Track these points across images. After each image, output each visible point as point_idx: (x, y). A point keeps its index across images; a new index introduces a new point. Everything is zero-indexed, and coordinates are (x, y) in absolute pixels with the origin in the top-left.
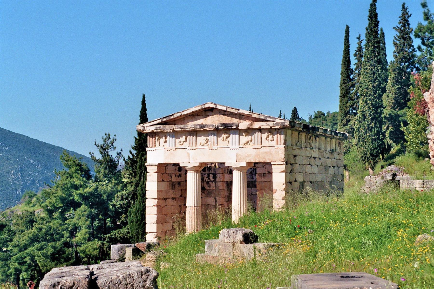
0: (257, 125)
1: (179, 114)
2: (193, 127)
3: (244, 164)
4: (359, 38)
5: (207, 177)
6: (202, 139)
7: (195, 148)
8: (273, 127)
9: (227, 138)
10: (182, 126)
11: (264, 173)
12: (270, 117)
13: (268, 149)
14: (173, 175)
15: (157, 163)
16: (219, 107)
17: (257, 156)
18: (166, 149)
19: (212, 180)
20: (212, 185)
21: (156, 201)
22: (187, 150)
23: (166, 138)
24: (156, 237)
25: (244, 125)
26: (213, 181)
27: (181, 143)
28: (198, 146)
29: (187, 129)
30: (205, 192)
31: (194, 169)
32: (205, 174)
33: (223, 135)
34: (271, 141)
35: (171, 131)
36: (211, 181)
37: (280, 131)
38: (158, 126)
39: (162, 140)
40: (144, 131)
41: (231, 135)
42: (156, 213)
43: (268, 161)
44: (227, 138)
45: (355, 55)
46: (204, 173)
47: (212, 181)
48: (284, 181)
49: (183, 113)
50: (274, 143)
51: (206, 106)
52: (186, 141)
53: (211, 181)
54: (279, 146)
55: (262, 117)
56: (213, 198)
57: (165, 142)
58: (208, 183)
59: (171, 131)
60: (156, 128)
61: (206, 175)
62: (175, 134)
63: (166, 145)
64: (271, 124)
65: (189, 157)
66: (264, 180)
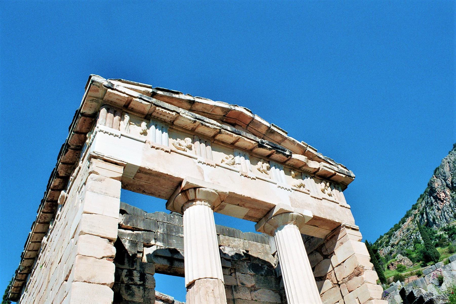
5: (126, 276)
11: (235, 284)
16: (257, 118)
19: (139, 283)
20: (138, 292)
23: (148, 127)
26: (140, 285)
27: (183, 148)
29: (207, 124)
31: (213, 200)
36: (135, 284)
39: (136, 130)
40: (109, 90)
42: (112, 279)
47: (139, 286)
49: (197, 100)
65: (202, 175)
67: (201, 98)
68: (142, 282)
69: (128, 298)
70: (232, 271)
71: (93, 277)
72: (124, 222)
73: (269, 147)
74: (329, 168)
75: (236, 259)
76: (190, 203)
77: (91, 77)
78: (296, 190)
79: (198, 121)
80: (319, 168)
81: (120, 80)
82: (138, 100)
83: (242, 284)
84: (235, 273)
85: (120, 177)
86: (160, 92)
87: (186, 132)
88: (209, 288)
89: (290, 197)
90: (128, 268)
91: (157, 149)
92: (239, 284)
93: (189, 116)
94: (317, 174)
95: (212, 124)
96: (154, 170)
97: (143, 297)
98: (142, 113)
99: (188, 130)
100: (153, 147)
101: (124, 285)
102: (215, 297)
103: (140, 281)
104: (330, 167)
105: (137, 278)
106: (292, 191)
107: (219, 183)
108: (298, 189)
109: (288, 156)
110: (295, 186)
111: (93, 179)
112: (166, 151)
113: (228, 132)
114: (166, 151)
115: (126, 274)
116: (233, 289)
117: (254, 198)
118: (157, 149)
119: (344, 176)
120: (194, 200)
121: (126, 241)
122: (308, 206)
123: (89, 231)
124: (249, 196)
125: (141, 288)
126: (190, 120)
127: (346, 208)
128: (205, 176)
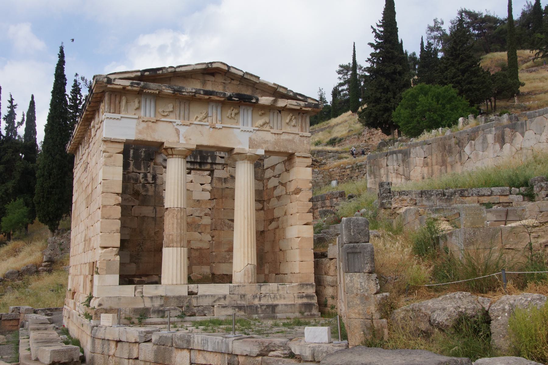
0: (282, 103)
1: (173, 69)
2: (194, 91)
3: (261, 152)
4: (11, 101)
5: (143, 178)
8: (304, 109)
9: (236, 114)
11: (226, 177)
12: (300, 95)
13: (290, 137)
15: (124, 138)
18: (141, 120)
19: (151, 182)
20: (151, 189)
21: (120, 198)
22: (175, 124)
24: (117, 255)
25: (265, 100)
26: (152, 183)
27: (166, 114)
29: (184, 93)
30: (140, 198)
31: (184, 153)
32: (139, 173)
33: (229, 112)
34: (294, 126)
35: (157, 92)
36: (149, 183)
37: (305, 115)
38: (134, 81)
40: (109, 86)
41: (241, 112)
42: (119, 216)
44: (236, 114)
45: (4, 119)
49: (178, 70)
53: (149, 183)
55: (291, 94)
56: (152, 208)
58: (144, 186)
59: (157, 92)
60: (132, 83)
61: (141, 175)
65: (178, 135)
66: (224, 186)
69: (144, 193)
71: (110, 216)
78: (258, 130)
80: (286, 105)
86: (147, 73)
88: (175, 213)
97: (155, 191)
98: (135, 91)
99: (171, 96)
100: (143, 121)
104: (296, 104)
105: (150, 179)
106: (255, 131)
109: (254, 103)
110: (257, 127)
112: (153, 122)
113: (201, 95)
114: (153, 122)
119: (310, 109)
120: (172, 155)
121: (141, 152)
122: (266, 142)
125: (153, 185)
128: (181, 136)
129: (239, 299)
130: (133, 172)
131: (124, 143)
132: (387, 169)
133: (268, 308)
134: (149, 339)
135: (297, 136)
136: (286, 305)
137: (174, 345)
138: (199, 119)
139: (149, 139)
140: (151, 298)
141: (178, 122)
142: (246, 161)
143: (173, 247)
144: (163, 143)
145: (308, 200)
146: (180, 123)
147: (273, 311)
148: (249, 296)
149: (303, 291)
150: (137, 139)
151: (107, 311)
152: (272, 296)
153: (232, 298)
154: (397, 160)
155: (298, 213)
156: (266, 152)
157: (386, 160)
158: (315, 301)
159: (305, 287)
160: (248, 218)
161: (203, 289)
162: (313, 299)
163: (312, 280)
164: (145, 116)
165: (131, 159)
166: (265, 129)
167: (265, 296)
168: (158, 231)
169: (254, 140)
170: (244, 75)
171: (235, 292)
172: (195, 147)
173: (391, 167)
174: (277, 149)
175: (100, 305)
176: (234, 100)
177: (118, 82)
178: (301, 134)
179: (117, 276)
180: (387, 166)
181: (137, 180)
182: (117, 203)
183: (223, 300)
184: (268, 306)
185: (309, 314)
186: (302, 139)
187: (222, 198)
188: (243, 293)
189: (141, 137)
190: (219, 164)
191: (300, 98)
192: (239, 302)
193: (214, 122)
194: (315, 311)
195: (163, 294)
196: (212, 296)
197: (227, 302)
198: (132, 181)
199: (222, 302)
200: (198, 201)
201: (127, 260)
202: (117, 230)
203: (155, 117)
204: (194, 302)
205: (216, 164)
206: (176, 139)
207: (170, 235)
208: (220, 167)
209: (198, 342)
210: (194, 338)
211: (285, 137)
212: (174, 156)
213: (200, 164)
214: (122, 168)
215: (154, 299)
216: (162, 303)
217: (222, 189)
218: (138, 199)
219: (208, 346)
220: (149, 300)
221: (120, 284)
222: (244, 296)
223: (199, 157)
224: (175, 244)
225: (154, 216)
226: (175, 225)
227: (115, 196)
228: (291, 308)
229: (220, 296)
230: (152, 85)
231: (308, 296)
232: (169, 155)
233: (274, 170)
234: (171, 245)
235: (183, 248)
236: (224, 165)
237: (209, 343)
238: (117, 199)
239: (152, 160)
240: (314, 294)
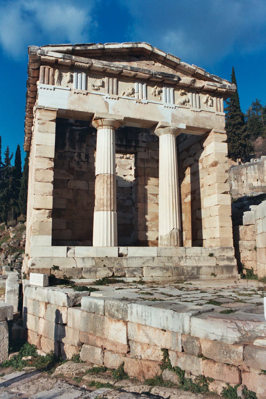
0: (200, 84)
2: (122, 66)
3: (183, 126)
5: (77, 156)
6: (126, 87)
7: (116, 97)
8: (219, 89)
10: (105, 62)
13: (208, 115)
14: (75, 131)
16: (157, 51)
17: (196, 119)
19: (85, 160)
21: (53, 164)
24: (49, 217)
25: (186, 80)
26: (85, 161)
27: (96, 88)
28: (120, 95)
32: (74, 153)
34: (210, 106)
35: (88, 65)
36: (82, 161)
40: (42, 57)
42: (52, 179)
43: (208, 128)
46: (73, 151)
48: (227, 152)
49: (106, 47)
50: (213, 109)
51: (140, 46)
52: (103, 86)
53: (82, 161)
54: (220, 113)
57: (71, 81)
60: (64, 56)
61: (76, 154)
62: (91, 72)
63: (73, 85)
64: (218, 85)
65: (108, 108)
66: (147, 165)
67: (110, 44)
68: (86, 160)
69: (78, 169)
70: (146, 149)
71: (43, 179)
72: (75, 122)
73: (160, 77)
74: (212, 86)
75: (150, 141)
76: (100, 127)
77: (29, 48)
79: (105, 67)
80: (204, 86)
81: (48, 46)
82: (62, 60)
83: (152, 158)
84: (148, 150)
85: (55, 119)
86: (78, 48)
87: (100, 74)
89: (173, 114)
90: (78, 152)
91: (78, 93)
92: (150, 158)
93: (99, 64)
94: (203, 89)
95: (116, 67)
96: (75, 110)
99: (101, 72)
100: (75, 93)
101: (76, 162)
102: (107, 184)
103: (85, 159)
104: (213, 84)
107: (118, 112)
108: (181, 106)
109: (176, 81)
111: (40, 124)
112: (84, 94)
114: (84, 94)
115: (76, 155)
116: (145, 161)
117: (143, 119)
118: (78, 93)
120: (102, 126)
121: (76, 135)
122: (187, 118)
123: (39, 156)
124: (139, 118)
125: (86, 163)
126: (99, 67)
127: (221, 115)
128: (110, 108)
129: (167, 261)
130: (69, 151)
131: (57, 111)
132: (247, 176)
133: (193, 269)
134: (78, 303)
135: (214, 115)
136: (210, 267)
137: (107, 314)
138: (126, 94)
139: (80, 110)
140: (83, 258)
141: (107, 95)
142: (169, 135)
143: (103, 210)
144: (93, 114)
145: (225, 171)
146: (109, 97)
147: (198, 273)
148: (176, 259)
149: (224, 254)
150: (68, 109)
151: (39, 271)
152: (197, 258)
153: (160, 260)
154: (254, 169)
155: (216, 183)
156: (186, 126)
157: (245, 170)
158: (235, 263)
159: (226, 250)
160: (172, 186)
161: (132, 251)
162: (233, 261)
163: (231, 243)
164: (77, 88)
165: (67, 140)
166: (186, 107)
167: (190, 258)
168: (91, 202)
169: (176, 115)
170: (166, 55)
171: (162, 255)
172: (123, 118)
173: (249, 175)
174: (196, 125)
175: (33, 265)
176: (159, 78)
177: (50, 54)
178: (217, 113)
179: (50, 238)
180: (247, 174)
181: (72, 158)
182: (50, 167)
183: (151, 261)
184: (193, 268)
185: (230, 275)
186: (218, 117)
187: (145, 176)
188: (170, 255)
189: (72, 108)
190: (142, 147)
191: (216, 80)
192: (166, 264)
193: (140, 98)
194: (235, 272)
195: (95, 256)
196: (141, 257)
197: (155, 264)
198: (68, 159)
199: (151, 264)
200: (122, 188)
201: (64, 226)
202: (50, 193)
203: (86, 89)
204: (125, 263)
205: (139, 147)
206: (106, 111)
207: (100, 199)
208: (142, 150)
209: (137, 314)
210: (131, 307)
211: (202, 114)
212: (104, 127)
213: (126, 146)
214: (55, 135)
215: (86, 260)
216: (94, 264)
217: (145, 168)
218: (73, 174)
219: (151, 320)
220: (81, 261)
221: (52, 245)
222: (171, 257)
223: (124, 141)
224: (105, 208)
225: (87, 189)
226: (105, 190)
227: (48, 161)
228: (214, 269)
229: (148, 258)
230: (83, 59)
231: (229, 259)
232: (99, 126)
233: (188, 151)
234: (102, 208)
235: (112, 212)
236: (147, 149)
237: (153, 316)
238: (49, 163)
239: (85, 142)
240: (234, 257)
